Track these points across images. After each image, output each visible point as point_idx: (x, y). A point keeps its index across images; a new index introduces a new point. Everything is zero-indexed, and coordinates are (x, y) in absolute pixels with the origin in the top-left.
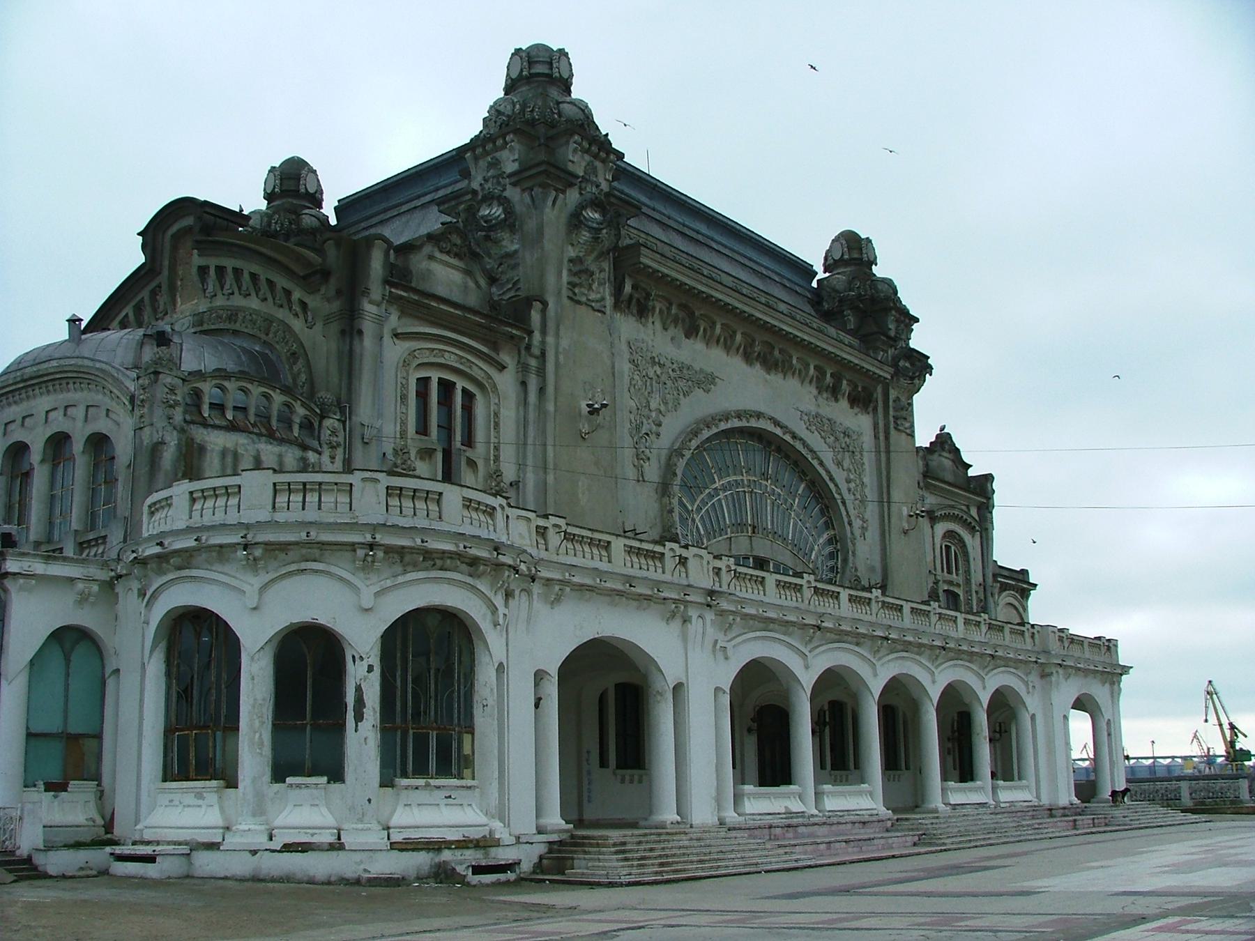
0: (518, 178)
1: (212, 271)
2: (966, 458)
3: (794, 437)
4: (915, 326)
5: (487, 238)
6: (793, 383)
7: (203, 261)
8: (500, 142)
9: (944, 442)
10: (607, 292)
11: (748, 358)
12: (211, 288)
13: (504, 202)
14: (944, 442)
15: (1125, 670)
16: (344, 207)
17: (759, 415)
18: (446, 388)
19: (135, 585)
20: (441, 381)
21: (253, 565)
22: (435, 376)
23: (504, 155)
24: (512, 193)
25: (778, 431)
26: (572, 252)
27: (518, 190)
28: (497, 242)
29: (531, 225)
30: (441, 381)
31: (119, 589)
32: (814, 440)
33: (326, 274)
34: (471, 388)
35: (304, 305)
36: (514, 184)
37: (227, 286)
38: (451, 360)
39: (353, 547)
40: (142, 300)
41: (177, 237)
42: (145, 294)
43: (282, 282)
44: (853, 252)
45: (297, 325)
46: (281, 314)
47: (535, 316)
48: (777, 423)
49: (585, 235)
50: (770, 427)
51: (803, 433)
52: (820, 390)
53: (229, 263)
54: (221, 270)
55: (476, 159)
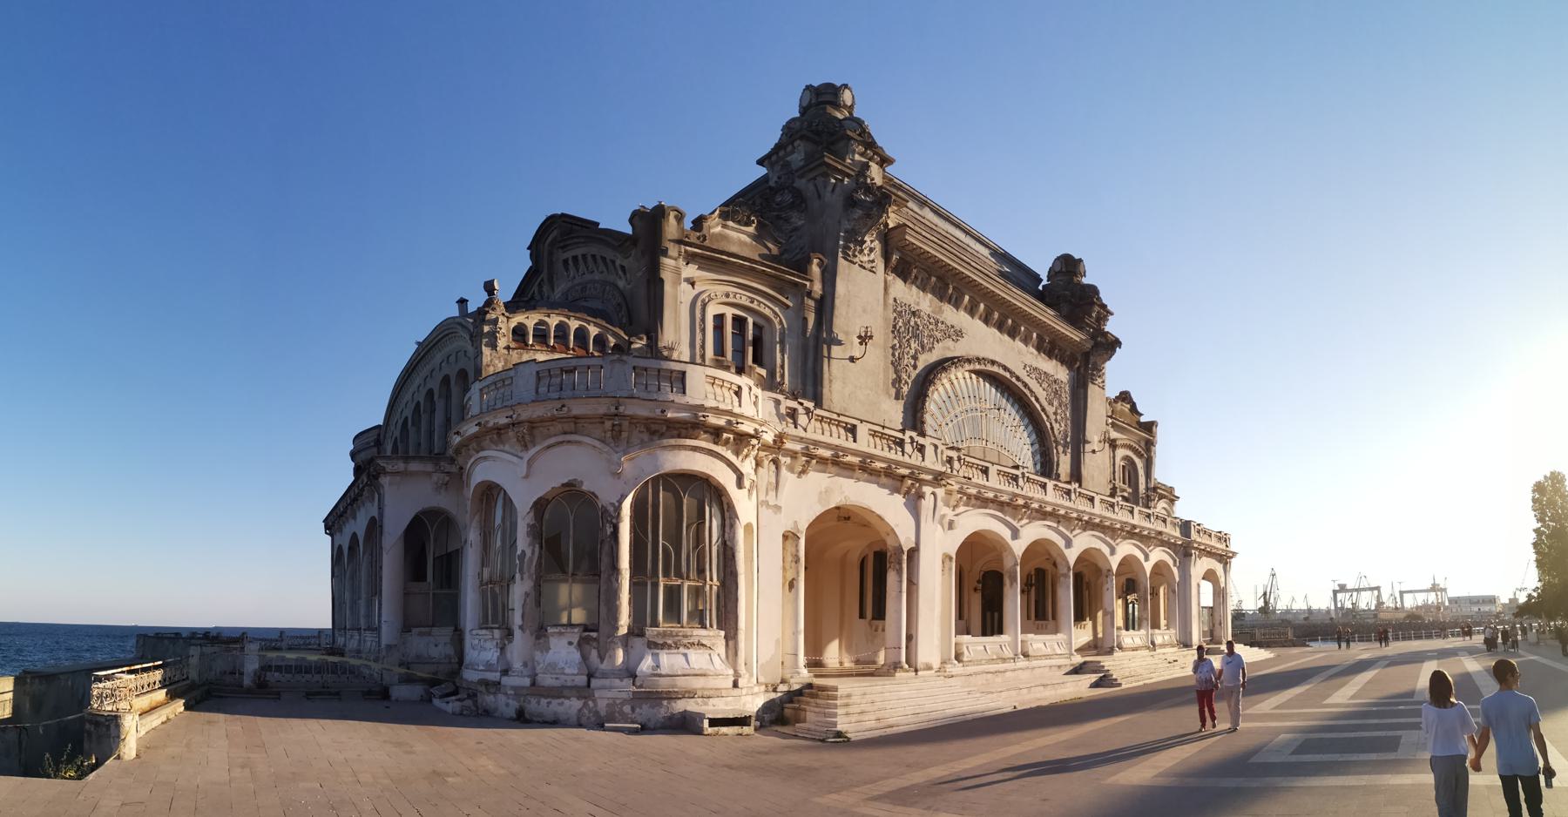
2: (1140, 409)
3: (1018, 379)
5: (778, 217)
6: (1019, 344)
8: (789, 148)
9: (1125, 397)
10: (877, 255)
14: (1125, 397)
15: (1234, 554)
17: (993, 362)
18: (739, 322)
20: (736, 319)
22: (729, 312)
25: (1007, 375)
26: (847, 225)
27: (804, 181)
28: (787, 220)
30: (736, 319)
32: (1033, 384)
34: (761, 322)
36: (801, 177)
38: (745, 301)
47: (815, 269)
48: (1006, 368)
49: (859, 213)
50: (1001, 371)
51: (1027, 380)
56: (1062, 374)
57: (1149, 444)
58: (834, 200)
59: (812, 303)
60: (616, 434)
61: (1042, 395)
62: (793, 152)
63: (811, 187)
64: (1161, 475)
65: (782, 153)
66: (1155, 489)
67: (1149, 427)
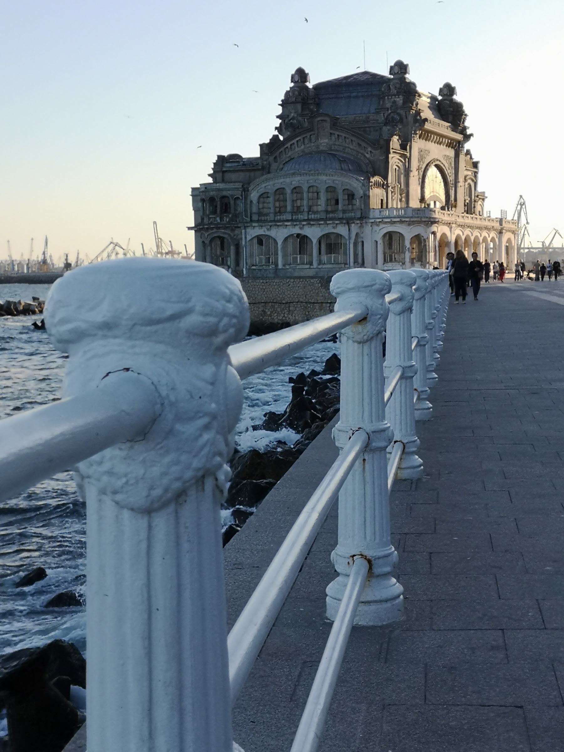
0: (402, 107)
1: (336, 136)
2: (473, 157)
4: (468, 118)
7: (332, 131)
8: (397, 97)
11: (435, 143)
12: (333, 138)
13: (399, 114)
16: (318, 87)
17: (437, 160)
19: (370, 225)
21: (409, 225)
22: (395, 167)
23: (398, 99)
24: (398, 111)
27: (402, 111)
29: (405, 120)
31: (364, 225)
32: (444, 162)
33: (381, 148)
35: (371, 152)
37: (340, 140)
39: (425, 221)
40: (307, 137)
41: (318, 121)
42: (308, 135)
43: (363, 144)
44: (448, 90)
45: (368, 156)
46: (362, 151)
47: (408, 147)
49: (417, 124)
52: (446, 146)
53: (344, 135)
54: (338, 135)
55: (388, 98)
56: (451, 153)
57: (476, 173)
58: (410, 119)
59: (407, 160)
60: (427, 224)
61: (447, 165)
62: (399, 98)
63: (404, 114)
64: (480, 189)
65: (393, 97)
66: (477, 196)
67: (475, 165)
